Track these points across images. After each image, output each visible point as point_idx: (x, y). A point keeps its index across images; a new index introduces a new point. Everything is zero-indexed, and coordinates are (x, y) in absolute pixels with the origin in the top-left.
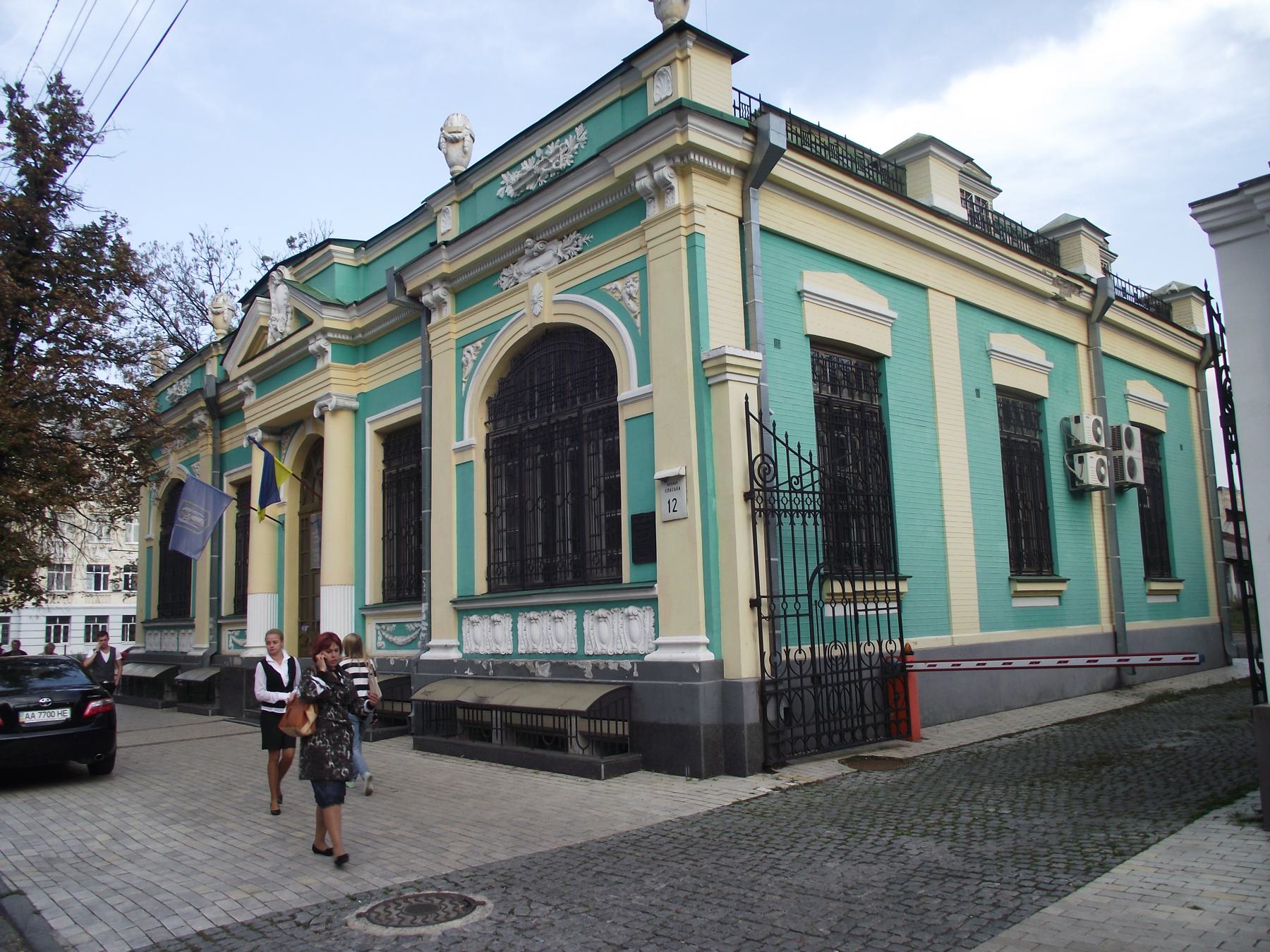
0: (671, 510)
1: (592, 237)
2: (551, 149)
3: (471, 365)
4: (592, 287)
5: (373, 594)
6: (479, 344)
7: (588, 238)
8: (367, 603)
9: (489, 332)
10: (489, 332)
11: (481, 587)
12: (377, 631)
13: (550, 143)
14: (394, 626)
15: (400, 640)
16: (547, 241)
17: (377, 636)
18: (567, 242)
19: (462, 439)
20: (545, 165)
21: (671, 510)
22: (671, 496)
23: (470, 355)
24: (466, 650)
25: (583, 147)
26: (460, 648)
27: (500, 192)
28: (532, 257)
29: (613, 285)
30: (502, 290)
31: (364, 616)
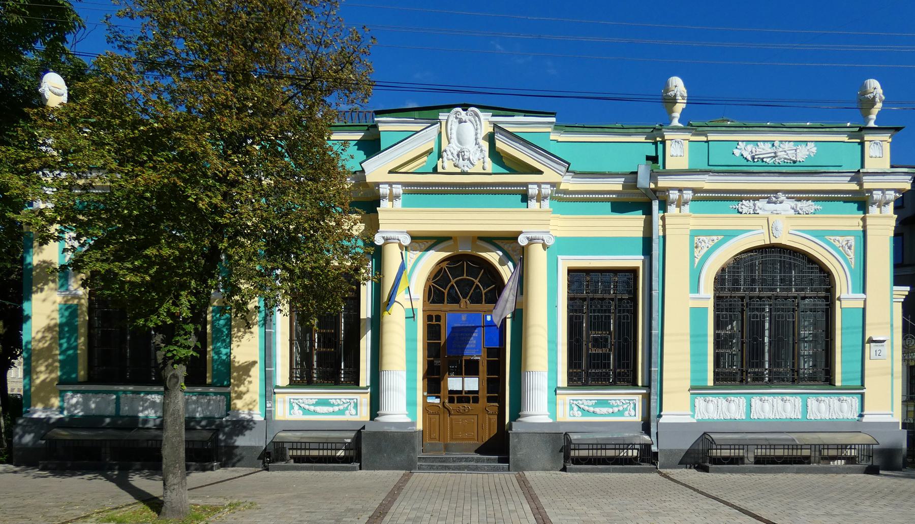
0: (878, 354)
1: (821, 208)
2: (787, 146)
3: (705, 250)
4: (820, 234)
5: (563, 380)
6: (715, 238)
7: (818, 207)
8: (560, 385)
9: (729, 235)
10: (729, 235)
11: (710, 383)
12: (571, 405)
13: (786, 141)
14: (594, 401)
15: (604, 410)
16: (788, 198)
17: (572, 409)
18: (799, 204)
19: (698, 291)
20: (783, 153)
21: (878, 354)
22: (878, 348)
23: (707, 242)
24: (699, 416)
25: (812, 156)
26: (693, 416)
27: (738, 153)
28: (775, 203)
29: (837, 238)
30: (741, 213)
31: (556, 394)
